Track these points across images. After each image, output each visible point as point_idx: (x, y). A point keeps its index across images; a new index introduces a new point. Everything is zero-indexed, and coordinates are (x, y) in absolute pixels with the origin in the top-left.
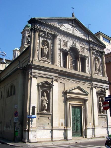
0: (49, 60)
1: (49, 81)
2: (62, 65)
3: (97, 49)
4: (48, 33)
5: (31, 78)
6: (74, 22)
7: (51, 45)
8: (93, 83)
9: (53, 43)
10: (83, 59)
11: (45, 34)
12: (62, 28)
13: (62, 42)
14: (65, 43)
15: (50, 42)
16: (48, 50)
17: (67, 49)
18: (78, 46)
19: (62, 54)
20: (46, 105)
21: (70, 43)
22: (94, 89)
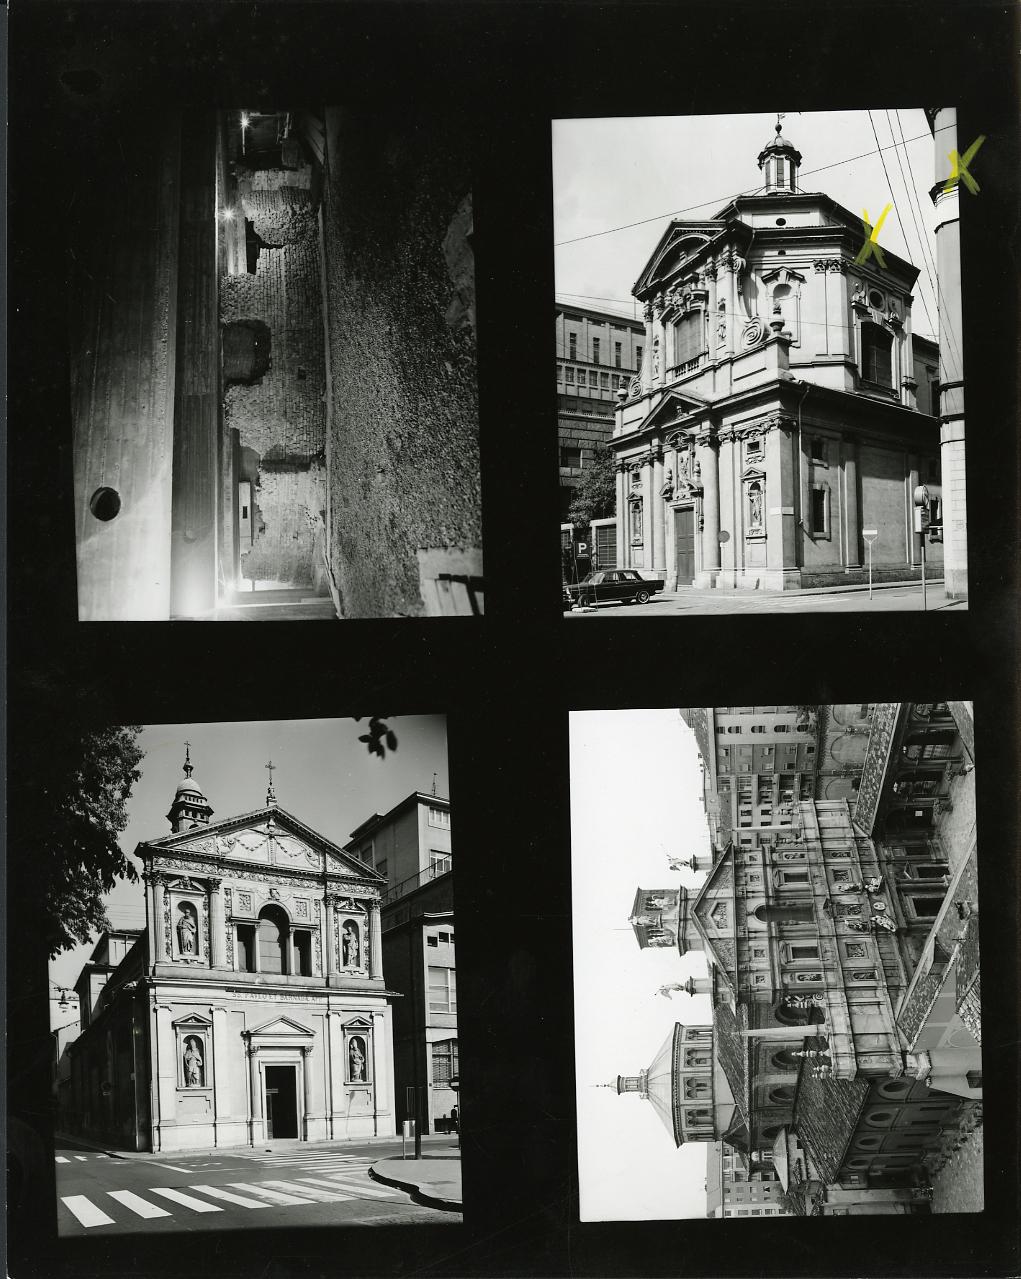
0: (202, 957)
1: (203, 1012)
2: (236, 967)
3: (353, 896)
4: (191, 879)
5: (155, 1010)
6: (272, 822)
7: (202, 913)
8: (332, 1000)
9: (208, 906)
10: (303, 939)
11: (185, 885)
12: (237, 854)
13: (236, 898)
14: (245, 896)
15: (198, 902)
16: (194, 931)
17: (252, 914)
18: (289, 897)
19: (235, 933)
20: (197, 1071)
21: (259, 892)
22: (333, 1017)
